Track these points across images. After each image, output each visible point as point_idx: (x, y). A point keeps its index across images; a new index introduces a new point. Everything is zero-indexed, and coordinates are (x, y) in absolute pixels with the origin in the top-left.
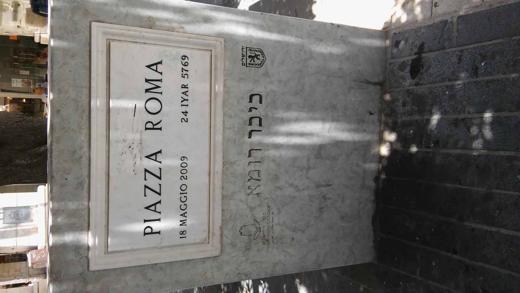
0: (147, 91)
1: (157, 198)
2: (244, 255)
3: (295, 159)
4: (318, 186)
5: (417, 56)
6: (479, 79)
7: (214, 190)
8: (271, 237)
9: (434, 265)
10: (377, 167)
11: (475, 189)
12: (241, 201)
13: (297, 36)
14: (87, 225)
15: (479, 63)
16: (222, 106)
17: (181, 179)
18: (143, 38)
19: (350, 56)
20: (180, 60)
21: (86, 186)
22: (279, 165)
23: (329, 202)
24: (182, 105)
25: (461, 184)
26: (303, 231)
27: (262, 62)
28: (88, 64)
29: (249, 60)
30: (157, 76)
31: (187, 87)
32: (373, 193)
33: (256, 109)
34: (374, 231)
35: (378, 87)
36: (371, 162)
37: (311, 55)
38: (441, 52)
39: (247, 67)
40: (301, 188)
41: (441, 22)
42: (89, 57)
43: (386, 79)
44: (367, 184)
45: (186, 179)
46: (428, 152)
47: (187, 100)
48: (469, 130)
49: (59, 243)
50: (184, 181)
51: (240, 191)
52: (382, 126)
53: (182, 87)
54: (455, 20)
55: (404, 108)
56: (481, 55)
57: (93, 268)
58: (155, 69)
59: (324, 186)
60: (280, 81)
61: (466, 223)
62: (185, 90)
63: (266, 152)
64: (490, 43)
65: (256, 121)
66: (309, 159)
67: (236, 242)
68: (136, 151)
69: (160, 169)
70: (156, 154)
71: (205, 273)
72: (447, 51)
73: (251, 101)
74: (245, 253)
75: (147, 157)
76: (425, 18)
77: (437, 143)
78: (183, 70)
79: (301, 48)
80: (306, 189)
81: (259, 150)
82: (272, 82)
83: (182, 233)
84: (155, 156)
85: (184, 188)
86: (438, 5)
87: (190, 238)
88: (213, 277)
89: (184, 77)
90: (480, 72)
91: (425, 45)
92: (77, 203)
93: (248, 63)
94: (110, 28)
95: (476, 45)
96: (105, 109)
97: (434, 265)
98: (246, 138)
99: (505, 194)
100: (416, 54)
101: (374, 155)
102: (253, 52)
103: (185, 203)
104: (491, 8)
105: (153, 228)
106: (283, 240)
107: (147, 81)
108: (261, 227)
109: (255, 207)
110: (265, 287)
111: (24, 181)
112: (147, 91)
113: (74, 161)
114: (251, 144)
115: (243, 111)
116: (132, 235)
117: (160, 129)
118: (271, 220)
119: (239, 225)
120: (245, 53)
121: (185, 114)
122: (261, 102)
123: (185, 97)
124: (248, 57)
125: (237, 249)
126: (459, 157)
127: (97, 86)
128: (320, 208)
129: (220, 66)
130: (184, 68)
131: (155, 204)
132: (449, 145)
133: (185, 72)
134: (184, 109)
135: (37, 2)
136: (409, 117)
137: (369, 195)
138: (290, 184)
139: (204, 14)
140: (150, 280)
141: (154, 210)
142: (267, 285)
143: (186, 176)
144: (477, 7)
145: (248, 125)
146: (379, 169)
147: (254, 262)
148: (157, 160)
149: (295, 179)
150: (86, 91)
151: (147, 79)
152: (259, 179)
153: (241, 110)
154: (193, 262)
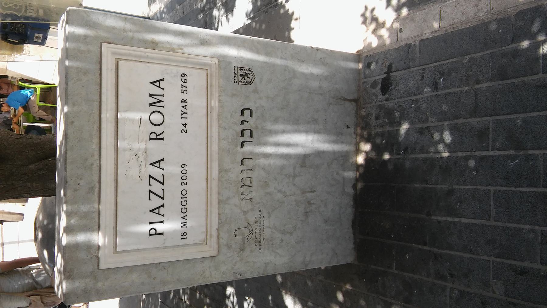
0: (151, 104)
1: (159, 202)
2: (239, 255)
3: (282, 168)
4: (304, 192)
5: (386, 75)
6: (439, 93)
7: (211, 195)
8: (262, 239)
9: (407, 257)
10: (355, 176)
11: (439, 186)
12: (235, 205)
13: (282, 58)
14: (97, 227)
15: (439, 79)
16: (218, 119)
17: (182, 185)
18: (148, 57)
19: (328, 76)
20: (179, 78)
21: (97, 190)
22: (268, 173)
23: (314, 207)
24: (182, 118)
25: (427, 184)
26: (291, 234)
27: (251, 80)
28: (99, 80)
29: (240, 78)
30: (160, 92)
31: (186, 101)
32: (352, 199)
33: (247, 122)
34: (354, 234)
35: (354, 103)
36: (349, 170)
37: (294, 74)
38: (407, 71)
39: (238, 84)
40: (288, 194)
41: (406, 45)
42: (99, 74)
43: (360, 97)
44: (346, 190)
45: (186, 185)
46: (399, 159)
47: (187, 113)
48: (432, 137)
49: (72, 243)
50: (184, 187)
51: (234, 196)
52: (358, 138)
53: (182, 102)
54: (417, 43)
55: (377, 121)
56: (440, 72)
57: (103, 266)
58: (158, 86)
59: (309, 192)
60: (268, 97)
61: (433, 217)
62: (184, 104)
63: (257, 161)
64: (447, 61)
65: (247, 133)
66: (294, 168)
67: (231, 243)
68: (141, 159)
69: (163, 175)
70: (159, 162)
71: (204, 272)
72: (411, 70)
73: (242, 115)
74: (240, 254)
75: (151, 164)
76: (392, 42)
77: (406, 149)
78: (183, 87)
79: (286, 68)
80: (293, 195)
81: (251, 159)
82: (260, 98)
83: (183, 234)
84: (158, 163)
85: (184, 192)
86: (402, 31)
87: (190, 239)
88: (211, 276)
89: (184, 93)
91: (393, 65)
92: (89, 206)
93: (239, 81)
94: (118, 49)
95: (436, 64)
96: (113, 121)
97: (407, 257)
98: (239, 148)
99: (464, 189)
100: (385, 73)
101: (352, 164)
102: (244, 71)
103: (185, 207)
104: (447, 32)
105: (157, 230)
106: (273, 242)
107: (151, 96)
108: (254, 229)
109: (248, 211)
110: (250, 302)
111: (24, 195)
112: (151, 104)
113: (86, 168)
114: (243, 153)
115: (236, 123)
116: (138, 235)
117: (163, 139)
118: (262, 223)
119: (233, 227)
120: (236, 72)
121: (185, 125)
122: (251, 116)
123: (185, 111)
124: (239, 76)
125: (232, 250)
126: (425, 160)
127: (107, 100)
128: (305, 213)
129: (215, 82)
130: (184, 84)
131: (159, 208)
132: (416, 150)
133: (184, 88)
134: (184, 121)
135: (6, 29)
136: (382, 128)
137: (348, 201)
138: (279, 191)
139: (201, 37)
140: (154, 278)
141: (158, 213)
142: (252, 300)
143: (186, 182)
144: (435, 32)
145: (241, 136)
146: (356, 177)
147: (248, 262)
148: (160, 167)
149: (283, 186)
150: (97, 104)
151: (151, 94)
152: (251, 185)
153: (234, 122)
154: (193, 262)
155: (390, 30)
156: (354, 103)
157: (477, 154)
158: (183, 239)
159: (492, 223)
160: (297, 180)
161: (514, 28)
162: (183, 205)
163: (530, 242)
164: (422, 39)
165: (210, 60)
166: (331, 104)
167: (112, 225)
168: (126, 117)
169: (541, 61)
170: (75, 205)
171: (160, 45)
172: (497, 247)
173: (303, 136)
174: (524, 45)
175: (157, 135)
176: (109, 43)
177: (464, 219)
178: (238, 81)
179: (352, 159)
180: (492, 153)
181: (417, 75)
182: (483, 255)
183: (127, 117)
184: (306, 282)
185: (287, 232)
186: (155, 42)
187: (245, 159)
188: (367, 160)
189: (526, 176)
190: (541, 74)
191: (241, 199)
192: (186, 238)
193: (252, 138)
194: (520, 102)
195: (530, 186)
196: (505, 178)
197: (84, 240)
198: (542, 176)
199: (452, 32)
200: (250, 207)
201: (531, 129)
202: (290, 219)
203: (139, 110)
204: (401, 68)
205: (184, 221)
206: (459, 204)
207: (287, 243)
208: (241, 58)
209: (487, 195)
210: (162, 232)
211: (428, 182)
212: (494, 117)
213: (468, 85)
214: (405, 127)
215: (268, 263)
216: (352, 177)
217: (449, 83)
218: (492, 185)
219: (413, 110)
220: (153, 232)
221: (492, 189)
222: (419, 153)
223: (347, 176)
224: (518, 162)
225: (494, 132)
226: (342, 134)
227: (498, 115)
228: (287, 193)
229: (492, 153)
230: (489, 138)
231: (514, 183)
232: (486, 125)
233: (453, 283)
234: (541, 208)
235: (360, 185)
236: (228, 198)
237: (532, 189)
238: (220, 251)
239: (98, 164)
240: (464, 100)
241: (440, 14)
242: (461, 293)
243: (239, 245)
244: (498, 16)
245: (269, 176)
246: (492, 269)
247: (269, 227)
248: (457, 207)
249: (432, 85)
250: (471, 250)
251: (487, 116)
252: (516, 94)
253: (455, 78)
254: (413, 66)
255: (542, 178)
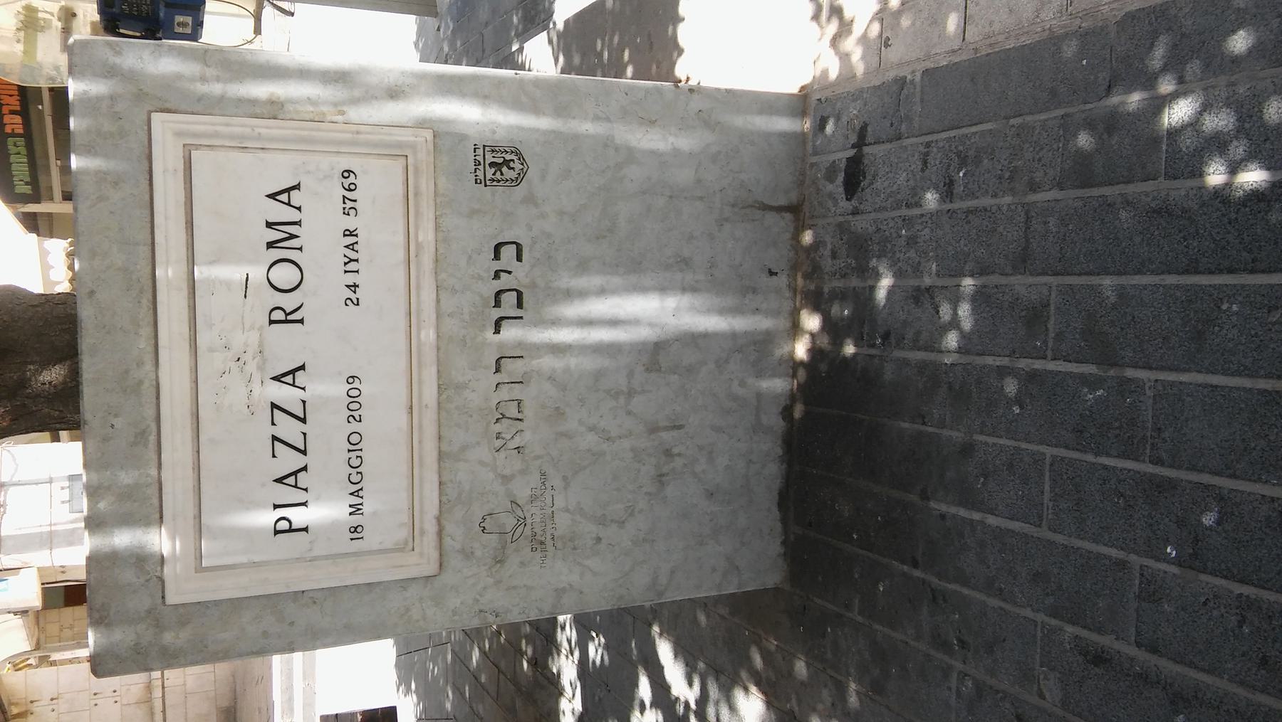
0: (270, 245)
1: (296, 461)
2: (491, 573)
3: (598, 375)
4: (653, 429)
5: (855, 151)
6: (955, 206)
7: (420, 442)
8: (549, 537)
9: (881, 589)
10: (789, 387)
11: (946, 433)
12: (481, 463)
13: (597, 118)
14: (158, 516)
15: (956, 170)
16: (433, 271)
17: (349, 422)
18: (259, 137)
19: (719, 152)
20: (337, 180)
21: (152, 438)
22: (563, 388)
23: (678, 462)
24: (346, 272)
25: (924, 423)
26: (621, 524)
27: (519, 174)
28: (147, 197)
29: (490, 172)
30: (291, 215)
31: (354, 233)
32: (779, 442)
33: (510, 273)
34: (784, 521)
35: (788, 216)
36: (774, 376)
37: (631, 156)
38: (895, 144)
39: (486, 186)
40: (613, 434)
41: (896, 80)
42: (148, 182)
43: (804, 198)
44: (764, 420)
45: (360, 421)
46: (871, 356)
47: (357, 260)
48: (938, 312)
49: (103, 551)
50: (355, 426)
51: (478, 443)
52: (798, 298)
53: (345, 235)
54: (918, 78)
55: (834, 262)
56: (958, 154)
57: (172, 599)
58: (287, 201)
59: (667, 429)
60: (561, 213)
61: (932, 504)
62: (351, 240)
63: (534, 362)
64: (974, 129)
65: (509, 299)
66: (631, 374)
67: (472, 547)
68: (251, 367)
69: (304, 402)
70: (293, 372)
71: (408, 610)
72: (904, 144)
73: (497, 256)
74: (494, 570)
75: (273, 378)
76: (869, 71)
77: (886, 337)
78: (346, 200)
79: (607, 143)
80: (627, 437)
81: (519, 357)
82: (543, 216)
83: (355, 529)
84: (291, 376)
85: (355, 439)
86: (890, 44)
87: (372, 539)
88: (424, 618)
89: (348, 214)
90: (958, 189)
91: (869, 129)
92: (137, 473)
93: (487, 178)
94: (188, 123)
95: (952, 133)
96: (184, 286)
97: (881, 589)
98: (489, 334)
99: (994, 444)
100: (853, 146)
101: (781, 361)
102: (499, 155)
103: (358, 470)
104: (978, 55)
105: (292, 521)
106: (576, 543)
107: (269, 225)
108: (528, 516)
109: (513, 476)
110: (599, 645)
111: (54, 426)
112: (270, 245)
113: (126, 391)
114: (501, 346)
115: (480, 278)
116: (249, 534)
117: (301, 321)
118: (549, 501)
119: (478, 512)
120: (480, 159)
121: (353, 289)
122: (519, 258)
123: (353, 255)
124: (487, 166)
125: (474, 561)
126: (922, 367)
127: (166, 240)
128: (658, 476)
129: (426, 186)
130: (348, 194)
131: (295, 473)
132: (906, 342)
133: (349, 204)
134: (351, 279)
135: (112, 8)
136: (843, 280)
137: (769, 447)
138: (589, 428)
139: (389, 82)
140: (292, 624)
141: (294, 484)
142: (603, 640)
143: (360, 416)
144: (954, 51)
145: (494, 307)
146: (792, 390)
147: (515, 588)
148: (296, 384)
149: (601, 417)
150: (144, 251)
151: (270, 221)
152: (520, 418)
153: (476, 276)
154: (382, 587)
155: (864, 39)
156: (788, 214)
157: (1023, 363)
158: (353, 541)
159: (1045, 533)
160: (638, 403)
161: (1113, 55)
162: (354, 466)
163: (1118, 590)
164: (928, 67)
165: (413, 135)
166: (727, 220)
167: (191, 512)
168: (213, 277)
169: (1164, 147)
170: (107, 471)
171: (289, 107)
172: (1052, 591)
173: (653, 298)
174: (1131, 103)
175: (288, 312)
176: (169, 111)
177: (989, 515)
178: (485, 180)
179: (782, 347)
180: (1052, 366)
181: (914, 156)
182: (1023, 607)
183: (215, 277)
184: (695, 618)
185: (612, 521)
186: (277, 100)
187: (506, 357)
188: (814, 351)
189: (1118, 432)
190: (1161, 179)
191: (495, 449)
192: (362, 538)
193: (522, 308)
194: (1115, 245)
195: (1123, 455)
196: (1074, 428)
197: (129, 544)
198: (1149, 434)
199: (988, 55)
200: (517, 464)
201: (1134, 317)
202: (618, 490)
203: (239, 260)
204: (884, 137)
205: (355, 500)
206: (982, 480)
207: (610, 544)
208: (492, 123)
209: (1039, 467)
210: (305, 527)
211: (926, 420)
212: (1060, 277)
213: (1013, 191)
214: (886, 282)
215: (564, 590)
216: (779, 391)
217: (976, 185)
218: (1050, 443)
219: (902, 242)
220: (283, 525)
221: (1049, 451)
222: (912, 349)
223: (767, 388)
224: (1103, 394)
225: (1059, 314)
226: (754, 291)
227: (1068, 274)
228: (610, 432)
229: (1052, 366)
230: (1047, 330)
231: (1092, 445)
232: (1044, 297)
233: (965, 663)
234: (1144, 513)
235: (798, 411)
236: (464, 448)
237: (1129, 464)
238: (445, 564)
239: (154, 383)
240: (1004, 228)
241: (966, 7)
242: (979, 688)
243: (491, 552)
244: (1082, 23)
245: (564, 396)
246: (1039, 642)
247: (567, 510)
248: (979, 486)
249: (943, 184)
250: (1001, 590)
251: (1047, 274)
252: (1108, 225)
253: (988, 173)
254: (907, 133)
255: (1150, 441)
